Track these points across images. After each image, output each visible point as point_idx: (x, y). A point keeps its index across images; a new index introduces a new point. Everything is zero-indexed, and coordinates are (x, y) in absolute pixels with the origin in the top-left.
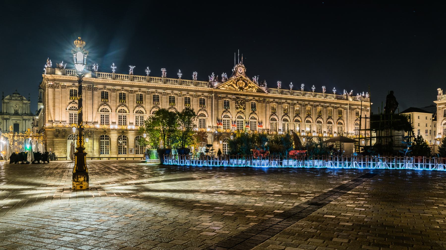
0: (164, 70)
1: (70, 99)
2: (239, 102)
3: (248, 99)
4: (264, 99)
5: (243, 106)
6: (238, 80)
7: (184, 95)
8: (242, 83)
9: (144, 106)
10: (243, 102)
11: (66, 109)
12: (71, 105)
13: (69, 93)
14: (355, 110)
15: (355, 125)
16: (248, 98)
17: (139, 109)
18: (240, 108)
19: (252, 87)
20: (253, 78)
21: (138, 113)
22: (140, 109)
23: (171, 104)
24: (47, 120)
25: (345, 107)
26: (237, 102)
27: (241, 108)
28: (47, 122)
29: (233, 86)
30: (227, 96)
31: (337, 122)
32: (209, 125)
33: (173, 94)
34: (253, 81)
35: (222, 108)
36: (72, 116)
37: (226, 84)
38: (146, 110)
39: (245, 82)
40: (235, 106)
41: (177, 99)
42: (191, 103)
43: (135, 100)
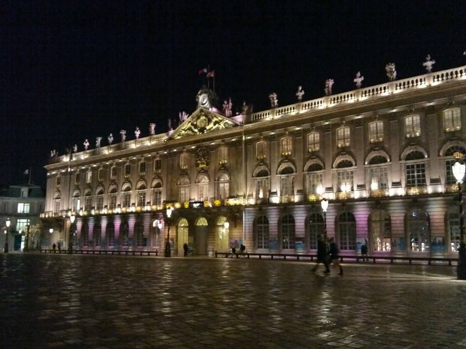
2: (200, 154)
5: (206, 159)
6: (199, 118)
37: (183, 130)
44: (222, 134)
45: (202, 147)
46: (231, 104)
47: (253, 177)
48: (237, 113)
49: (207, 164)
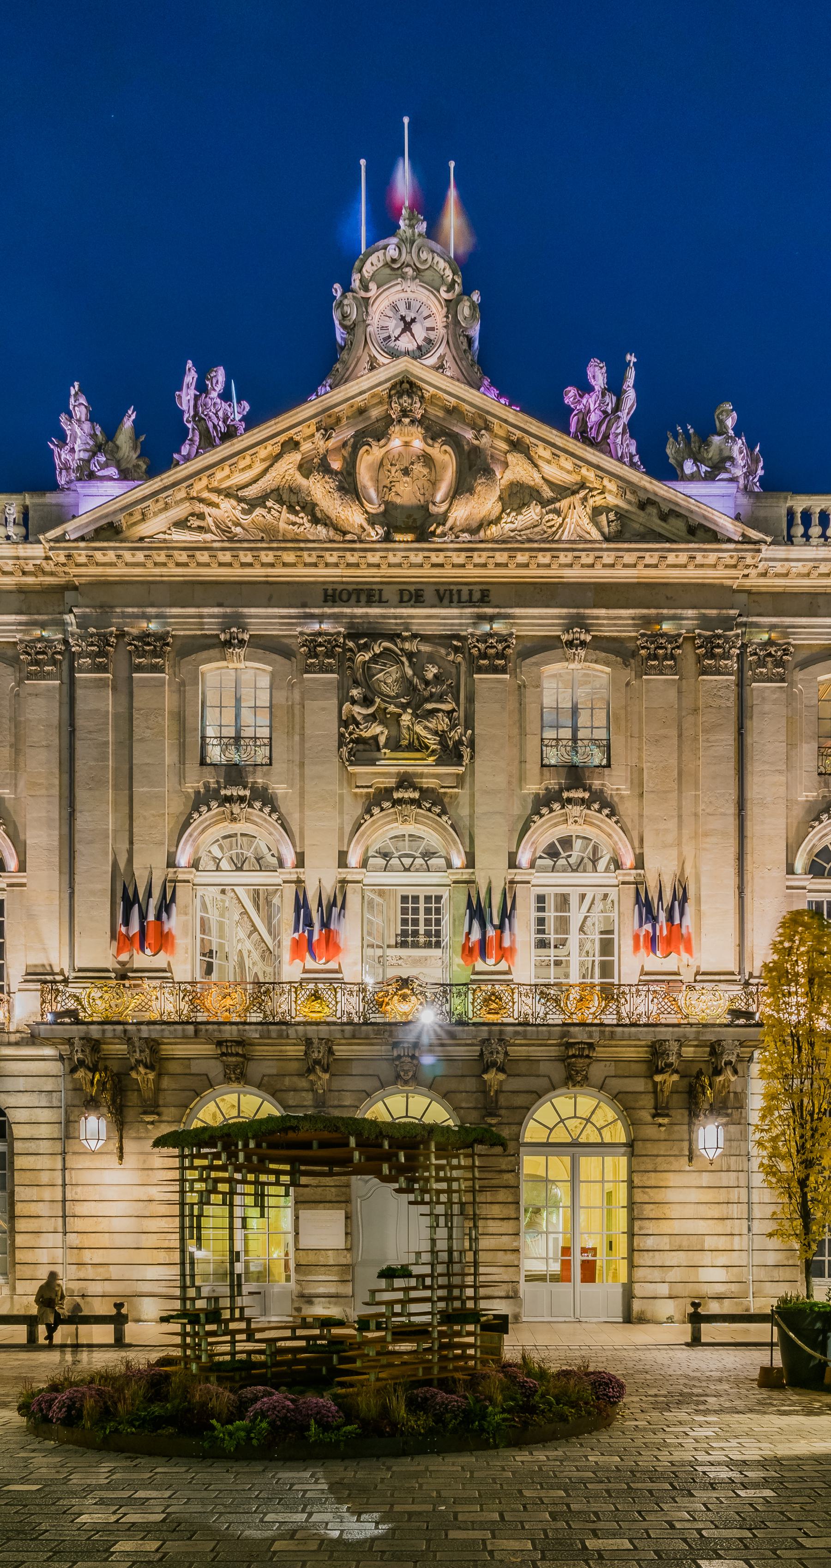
4: (705, 622)
5: (441, 723)
8: (427, 460)
10: (431, 671)
16: (498, 627)
18: (395, 745)
19: (547, 493)
20: (571, 395)
26: (356, 683)
27: (410, 748)
29: (310, 509)
35: (182, 761)
39: (454, 441)
40: (333, 727)
44: (574, 574)
45: (393, 637)
46: (630, 397)
48: (689, 467)
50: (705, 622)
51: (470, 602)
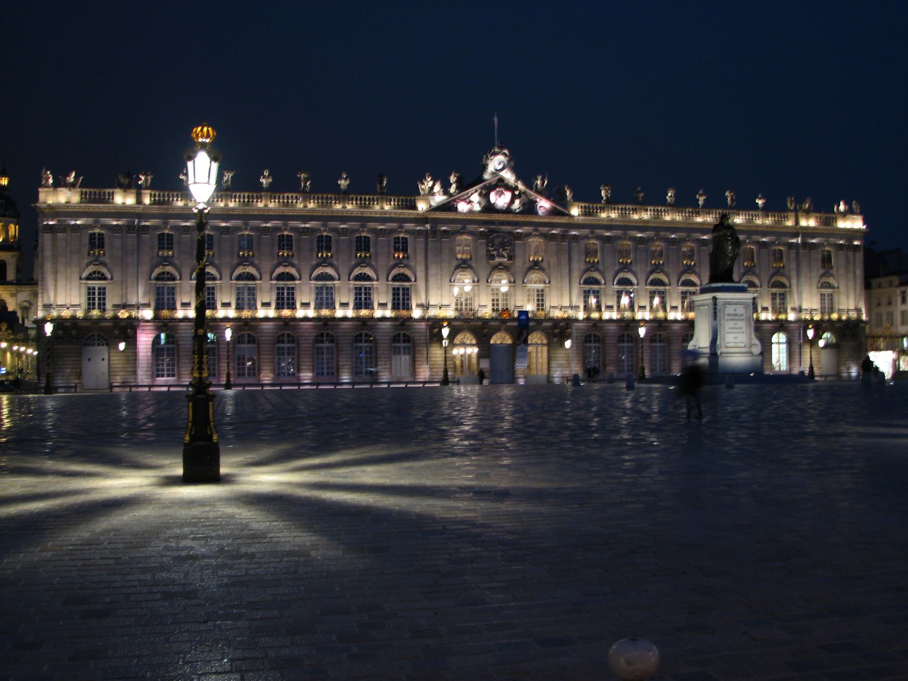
0: (305, 176)
1: (89, 254)
2: (497, 241)
3: (521, 233)
7: (353, 231)
9: (256, 262)
11: (81, 279)
12: (91, 269)
13: (86, 241)
14: (820, 250)
15: (822, 287)
17: (244, 271)
21: (242, 280)
22: (247, 270)
23: (322, 255)
24: (40, 304)
25: (792, 241)
26: (490, 242)
28: (40, 308)
30: (464, 228)
31: (769, 282)
32: (419, 302)
33: (326, 230)
34: (534, 187)
36: (94, 294)
38: (263, 271)
41: (337, 241)
42: (371, 250)
43: (236, 249)
45: (498, 232)
47: (580, 284)
49: (510, 258)
50: (564, 231)
51: (513, 225)
